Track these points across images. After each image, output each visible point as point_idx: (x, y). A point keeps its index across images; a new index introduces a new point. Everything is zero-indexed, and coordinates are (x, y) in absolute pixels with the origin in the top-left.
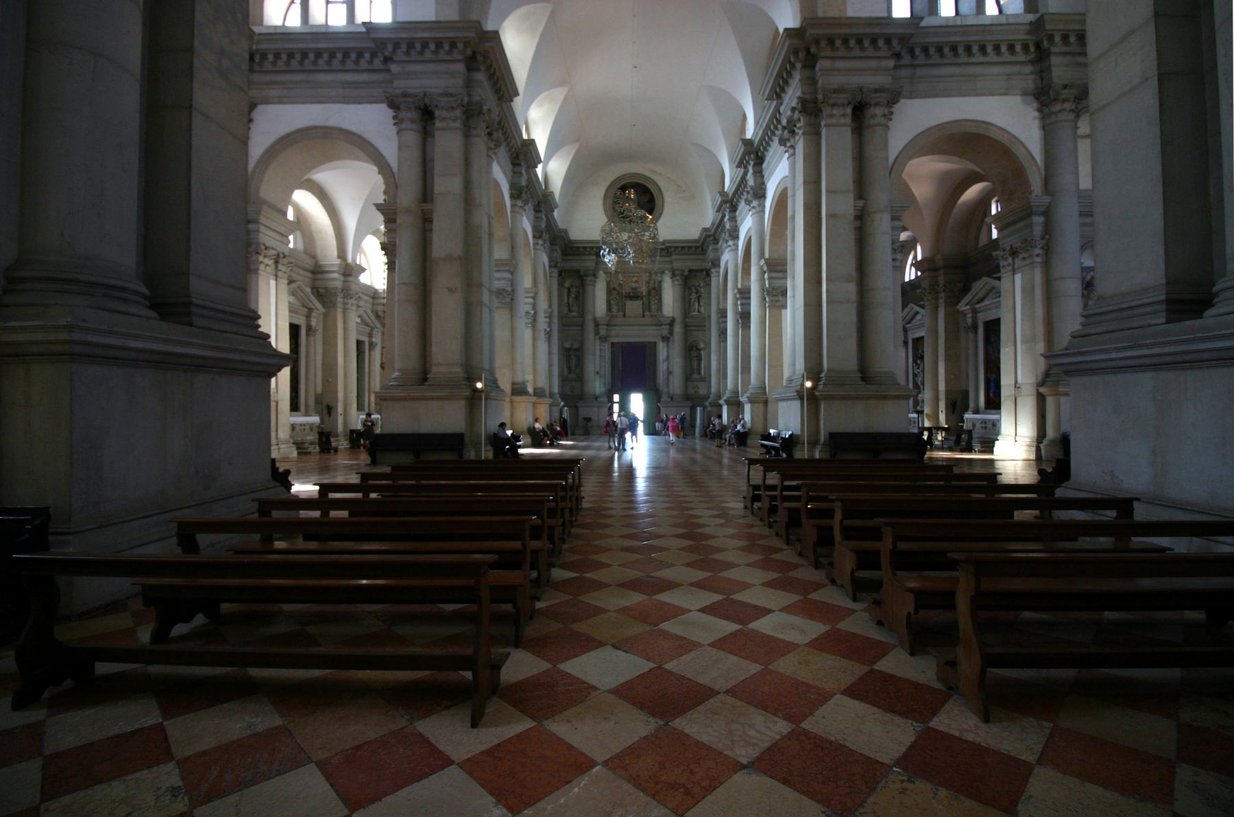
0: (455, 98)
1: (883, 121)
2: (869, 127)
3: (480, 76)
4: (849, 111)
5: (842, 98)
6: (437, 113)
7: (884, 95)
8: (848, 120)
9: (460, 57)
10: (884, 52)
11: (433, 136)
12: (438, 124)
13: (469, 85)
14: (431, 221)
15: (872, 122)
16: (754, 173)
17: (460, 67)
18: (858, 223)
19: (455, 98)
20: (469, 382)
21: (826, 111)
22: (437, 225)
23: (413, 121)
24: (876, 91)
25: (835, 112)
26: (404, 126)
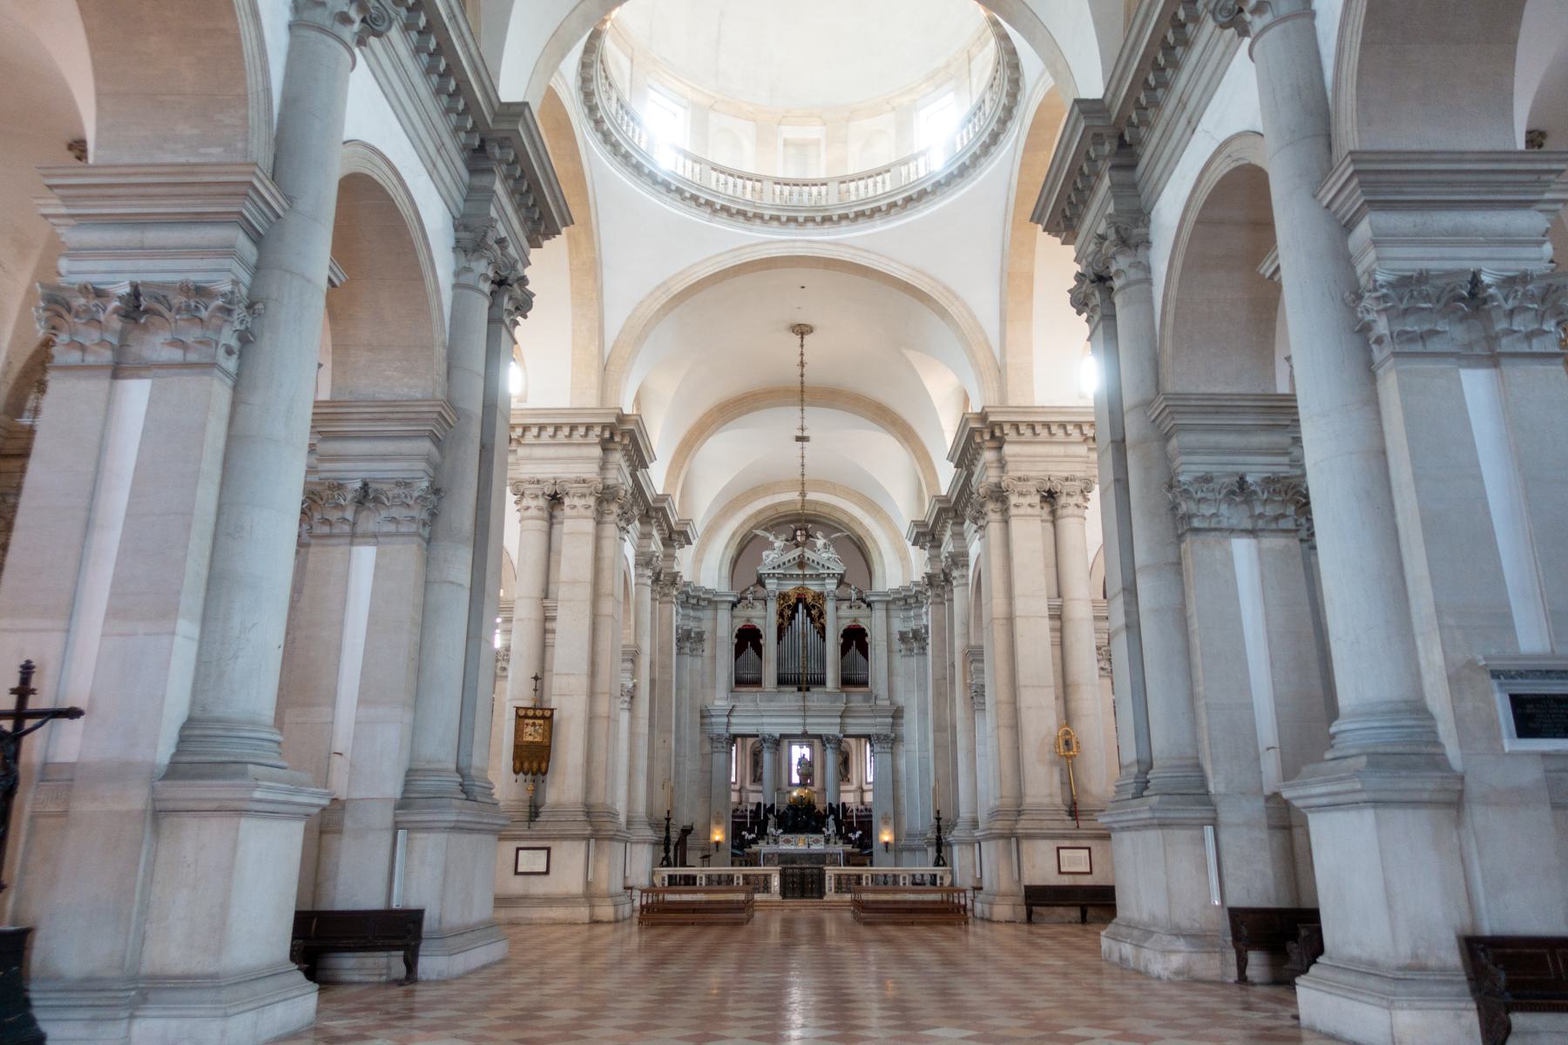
1: (1077, 511)
2: (1063, 517)
3: (618, 457)
4: (1036, 499)
5: (1031, 486)
6: (567, 501)
7: (1077, 483)
8: (1037, 510)
10: (1075, 434)
11: (562, 523)
12: (567, 511)
13: (603, 467)
14: (554, 619)
15: (1065, 512)
16: (954, 535)
17: (597, 451)
18: (1057, 624)
20: (588, 817)
21: (1014, 499)
22: (558, 626)
23: (540, 509)
24: (1067, 479)
25: (1022, 500)
26: (528, 513)
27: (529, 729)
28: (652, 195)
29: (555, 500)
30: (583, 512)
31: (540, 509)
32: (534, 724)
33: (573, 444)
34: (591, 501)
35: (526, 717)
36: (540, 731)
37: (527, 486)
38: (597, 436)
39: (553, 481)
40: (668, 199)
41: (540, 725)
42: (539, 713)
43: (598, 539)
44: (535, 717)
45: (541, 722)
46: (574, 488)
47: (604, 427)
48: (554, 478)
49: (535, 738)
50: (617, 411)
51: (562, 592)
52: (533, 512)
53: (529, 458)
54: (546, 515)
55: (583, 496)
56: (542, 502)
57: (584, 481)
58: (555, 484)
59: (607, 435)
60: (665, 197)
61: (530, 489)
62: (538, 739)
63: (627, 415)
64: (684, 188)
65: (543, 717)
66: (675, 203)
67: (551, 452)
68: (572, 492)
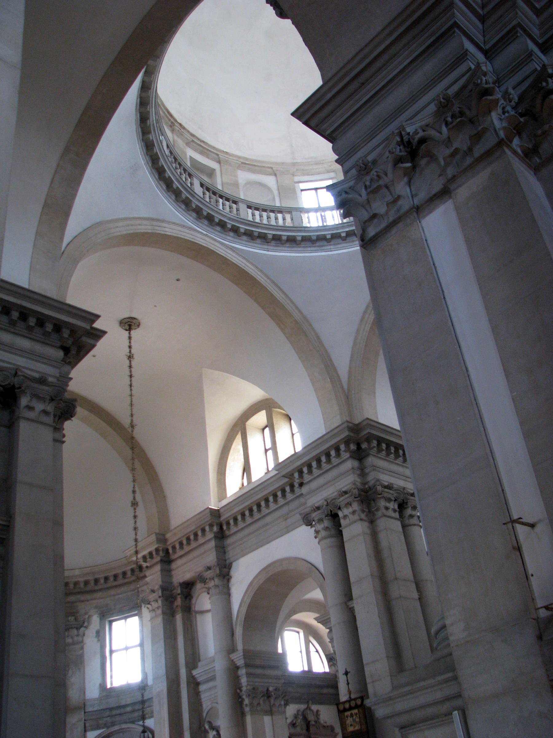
0: (350, 494)
6: (341, 514)
9: (347, 455)
12: (343, 522)
13: (362, 472)
17: (350, 464)
19: (350, 494)
23: (326, 529)
27: (349, 721)
28: (316, 251)
29: (334, 517)
30: (351, 516)
31: (326, 529)
32: (352, 715)
33: (335, 466)
34: (355, 506)
35: (345, 710)
36: (357, 720)
37: (314, 515)
38: (345, 451)
39: (325, 503)
40: (332, 247)
41: (356, 714)
42: (353, 704)
43: (374, 535)
44: (351, 708)
45: (356, 711)
46: (342, 501)
47: (347, 441)
48: (326, 500)
49: (354, 727)
50: (346, 424)
51: (355, 591)
52: (323, 533)
53: (311, 492)
54: (333, 532)
55: (349, 504)
56: (327, 523)
57: (346, 493)
58: (327, 505)
59: (353, 447)
60: (329, 247)
61: (315, 515)
62: (357, 728)
63: (360, 424)
64: (339, 231)
65: (357, 707)
66: (339, 246)
67: (321, 481)
68: (342, 504)
